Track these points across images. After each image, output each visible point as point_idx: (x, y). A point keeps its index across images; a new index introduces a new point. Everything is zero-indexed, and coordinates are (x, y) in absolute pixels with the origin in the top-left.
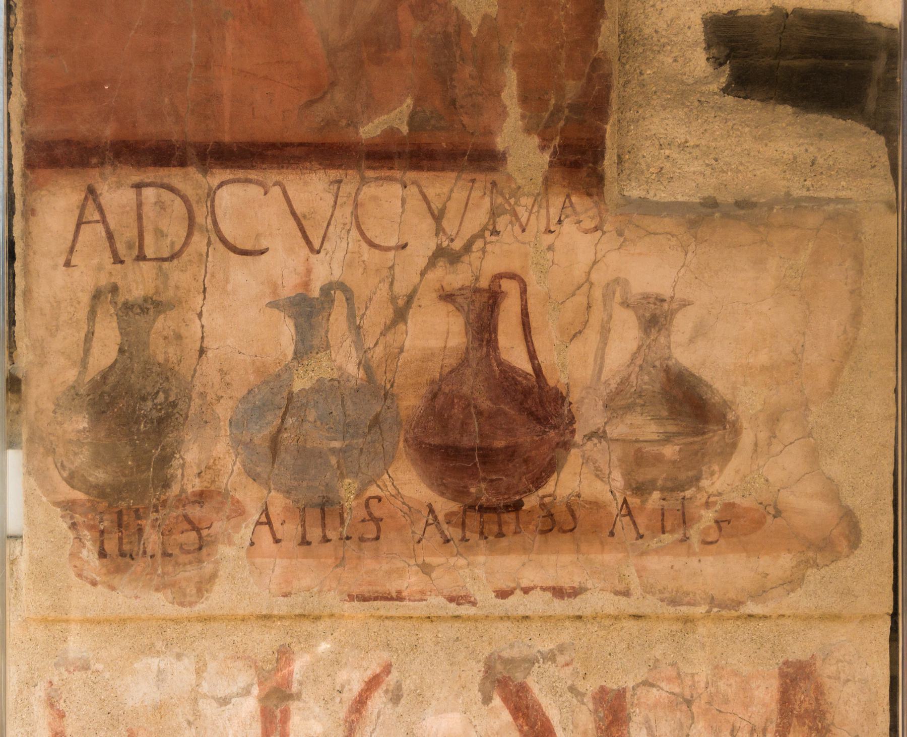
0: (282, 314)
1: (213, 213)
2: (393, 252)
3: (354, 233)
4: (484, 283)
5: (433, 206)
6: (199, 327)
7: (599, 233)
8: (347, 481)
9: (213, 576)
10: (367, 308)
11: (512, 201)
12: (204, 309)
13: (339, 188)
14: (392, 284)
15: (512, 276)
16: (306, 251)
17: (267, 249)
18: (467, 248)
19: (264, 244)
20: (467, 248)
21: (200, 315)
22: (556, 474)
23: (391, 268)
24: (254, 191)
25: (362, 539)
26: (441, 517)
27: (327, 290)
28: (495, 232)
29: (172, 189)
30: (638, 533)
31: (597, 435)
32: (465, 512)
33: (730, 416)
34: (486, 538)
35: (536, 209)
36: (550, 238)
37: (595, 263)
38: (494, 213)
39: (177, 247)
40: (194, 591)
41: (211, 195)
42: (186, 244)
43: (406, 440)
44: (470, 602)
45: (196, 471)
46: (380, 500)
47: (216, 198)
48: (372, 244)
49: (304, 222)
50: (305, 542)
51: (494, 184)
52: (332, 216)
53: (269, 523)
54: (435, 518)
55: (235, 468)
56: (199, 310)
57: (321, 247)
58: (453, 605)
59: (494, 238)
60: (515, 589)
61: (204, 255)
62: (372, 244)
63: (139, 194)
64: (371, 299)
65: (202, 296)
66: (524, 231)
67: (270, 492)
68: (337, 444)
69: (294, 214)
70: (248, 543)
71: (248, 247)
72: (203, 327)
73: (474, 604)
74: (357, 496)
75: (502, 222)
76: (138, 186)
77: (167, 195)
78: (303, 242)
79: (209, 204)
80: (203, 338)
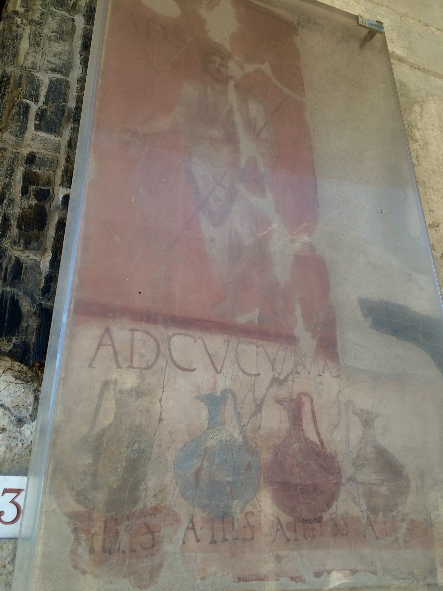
0: (202, 403)
1: (170, 348)
2: (254, 377)
3: (236, 366)
4: (294, 397)
5: (271, 358)
6: (159, 406)
7: (339, 379)
8: (236, 502)
9: (161, 566)
10: (243, 404)
11: (303, 359)
12: (163, 397)
13: (228, 344)
14: (254, 393)
15: (307, 395)
16: (213, 372)
17: (195, 369)
18: (286, 379)
19: (194, 366)
20: (286, 379)
21: (160, 400)
22: (336, 501)
23: (253, 385)
24: (189, 340)
25: (244, 539)
26: (284, 526)
27: (224, 392)
28: (297, 373)
29: (150, 335)
30: (376, 536)
31: (351, 479)
32: (295, 522)
33: (405, 473)
34: (307, 539)
35: (313, 364)
36: (320, 378)
37: (340, 392)
38: (296, 364)
39: (150, 363)
40: (148, 577)
41: (169, 339)
42: (155, 362)
43: (264, 478)
44: (302, 581)
45: (153, 494)
46: (253, 515)
47: (171, 341)
48: (244, 372)
49: (213, 358)
50: (213, 542)
51: (295, 350)
52: (226, 356)
53: (193, 528)
54: (281, 526)
55: (176, 492)
56: (160, 398)
57: (221, 371)
58: (293, 583)
59: (297, 376)
60: (324, 571)
61: (164, 368)
62: (244, 372)
63: (133, 335)
64: (245, 399)
65: (161, 390)
66: (309, 374)
67: (194, 508)
68: (230, 479)
69: (208, 354)
70: (181, 542)
71: (186, 367)
72: (161, 406)
73: (304, 581)
74: (241, 511)
75: (300, 368)
76: (132, 330)
77: (146, 337)
78: (212, 367)
79: (168, 343)
80: (161, 413)
